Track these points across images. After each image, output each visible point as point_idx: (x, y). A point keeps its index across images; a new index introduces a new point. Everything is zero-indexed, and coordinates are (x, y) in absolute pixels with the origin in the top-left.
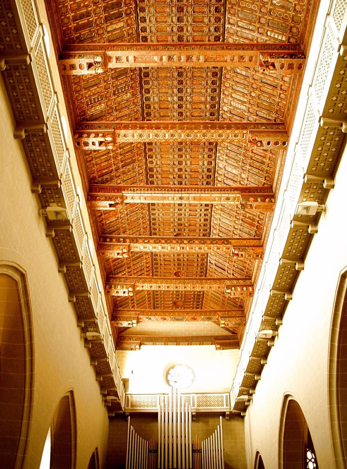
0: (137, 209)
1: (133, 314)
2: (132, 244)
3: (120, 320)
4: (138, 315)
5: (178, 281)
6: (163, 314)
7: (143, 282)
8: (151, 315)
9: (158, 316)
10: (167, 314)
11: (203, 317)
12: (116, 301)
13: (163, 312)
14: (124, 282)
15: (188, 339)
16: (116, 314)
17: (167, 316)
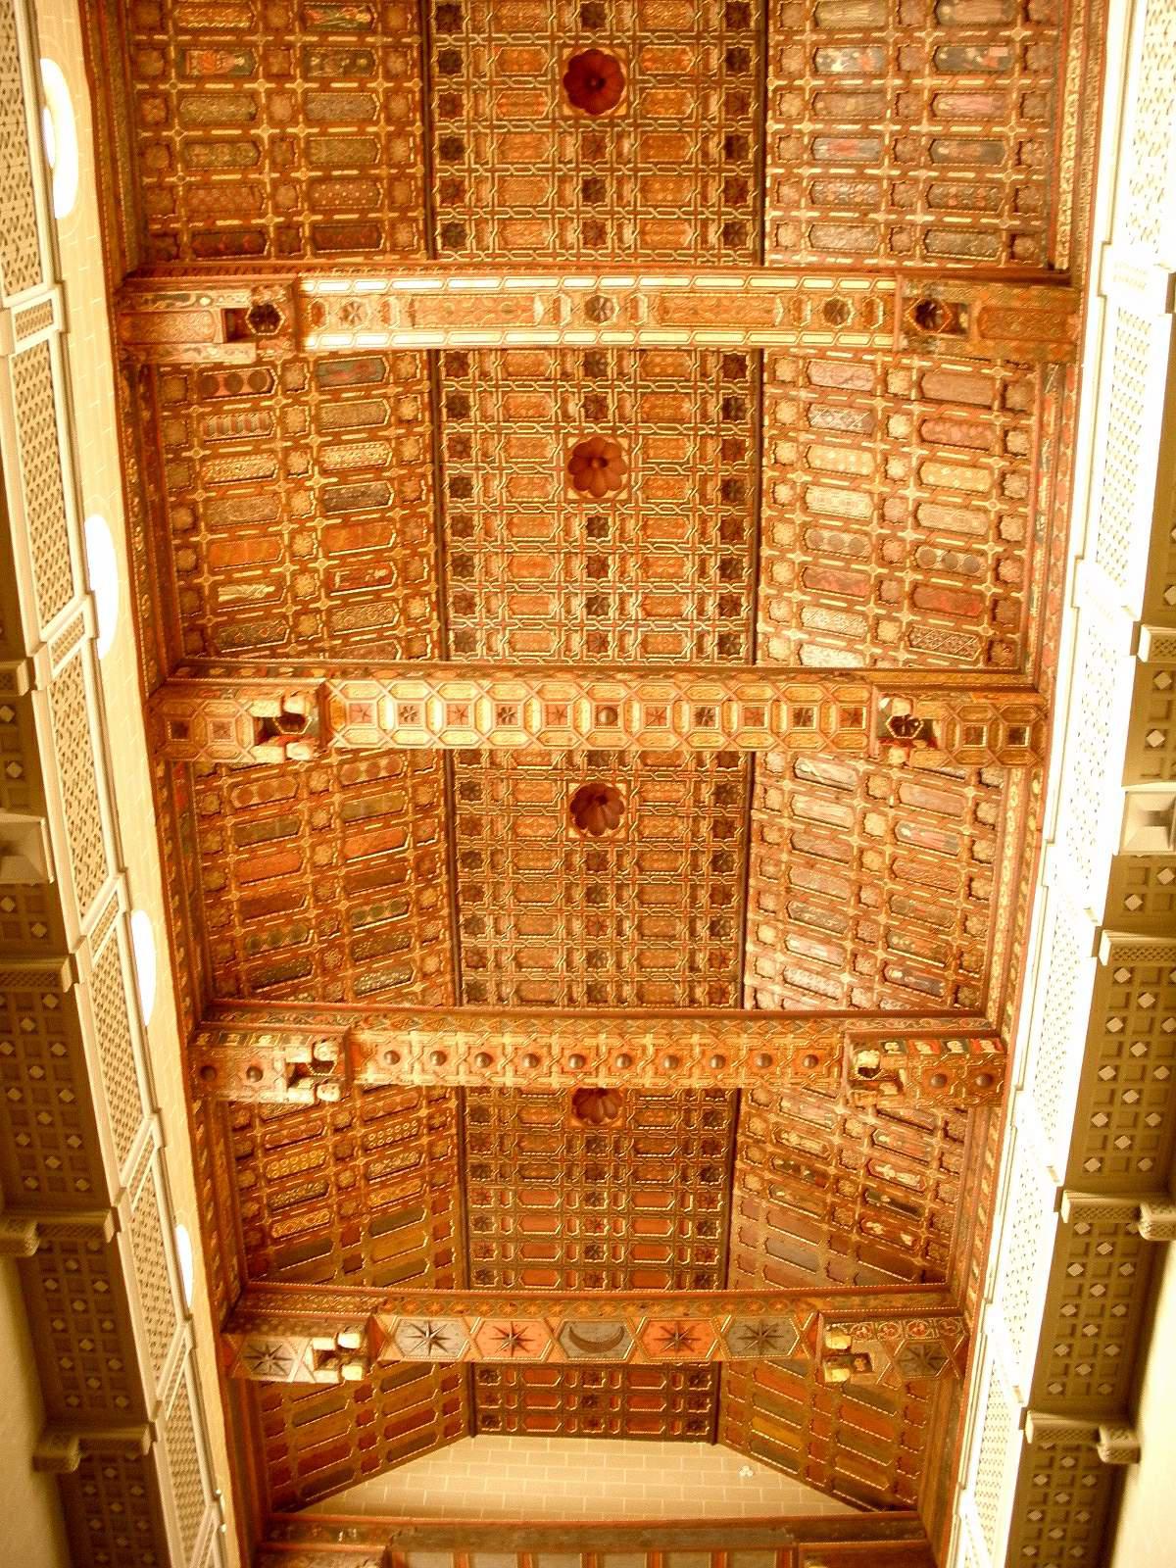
0: (382, 573)
1: (345, 1306)
2: (336, 686)
3: (274, 1328)
4: (375, 1310)
5: (586, 1025)
6: (508, 1309)
7: (395, 1027)
8: (443, 1311)
9: (483, 1314)
10: (533, 1309)
11: (727, 1319)
12: (263, 1244)
13: (511, 1300)
14: (297, 1021)
15: (647, 1535)
16: (255, 1306)
17: (532, 1316)
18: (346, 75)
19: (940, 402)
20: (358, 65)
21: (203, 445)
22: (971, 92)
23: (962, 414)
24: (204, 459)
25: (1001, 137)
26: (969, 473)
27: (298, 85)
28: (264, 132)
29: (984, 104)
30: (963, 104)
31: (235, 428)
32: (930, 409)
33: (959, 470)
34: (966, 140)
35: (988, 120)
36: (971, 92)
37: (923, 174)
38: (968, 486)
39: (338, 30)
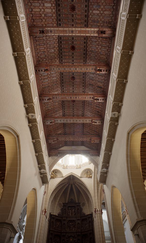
18: (93, 50)
19: (40, 19)
20: (92, 51)
21: (110, 16)
22: (42, 50)
23: (38, 18)
24: (111, 14)
25: (39, 46)
26: (35, 11)
27: (97, 50)
28: (100, 47)
29: (41, 49)
30: (42, 49)
31: (107, 17)
32: (41, 18)
33: (37, 11)
34: (41, 46)
35: (40, 47)
36: (42, 50)
37: (45, 42)
38: (35, 9)
39: (93, 54)
